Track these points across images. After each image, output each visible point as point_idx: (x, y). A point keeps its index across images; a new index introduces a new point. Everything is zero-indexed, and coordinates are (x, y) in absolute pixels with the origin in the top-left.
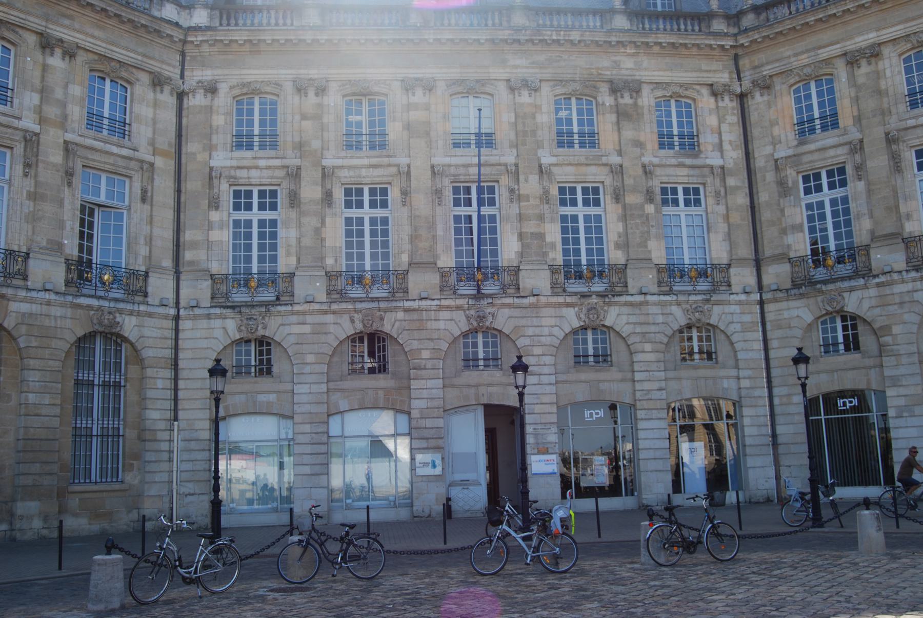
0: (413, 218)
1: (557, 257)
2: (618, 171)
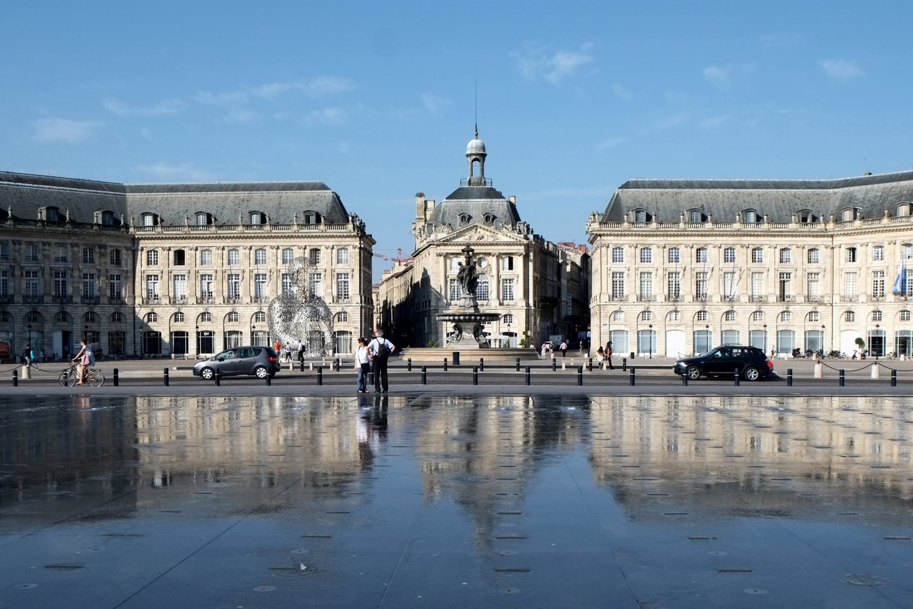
0: (45, 281)
1: (82, 293)
2: (99, 271)
